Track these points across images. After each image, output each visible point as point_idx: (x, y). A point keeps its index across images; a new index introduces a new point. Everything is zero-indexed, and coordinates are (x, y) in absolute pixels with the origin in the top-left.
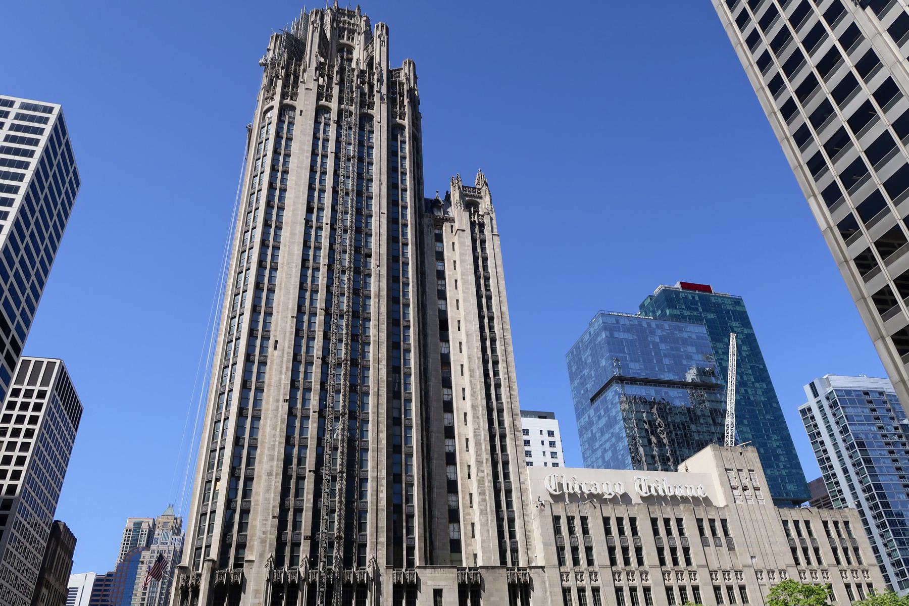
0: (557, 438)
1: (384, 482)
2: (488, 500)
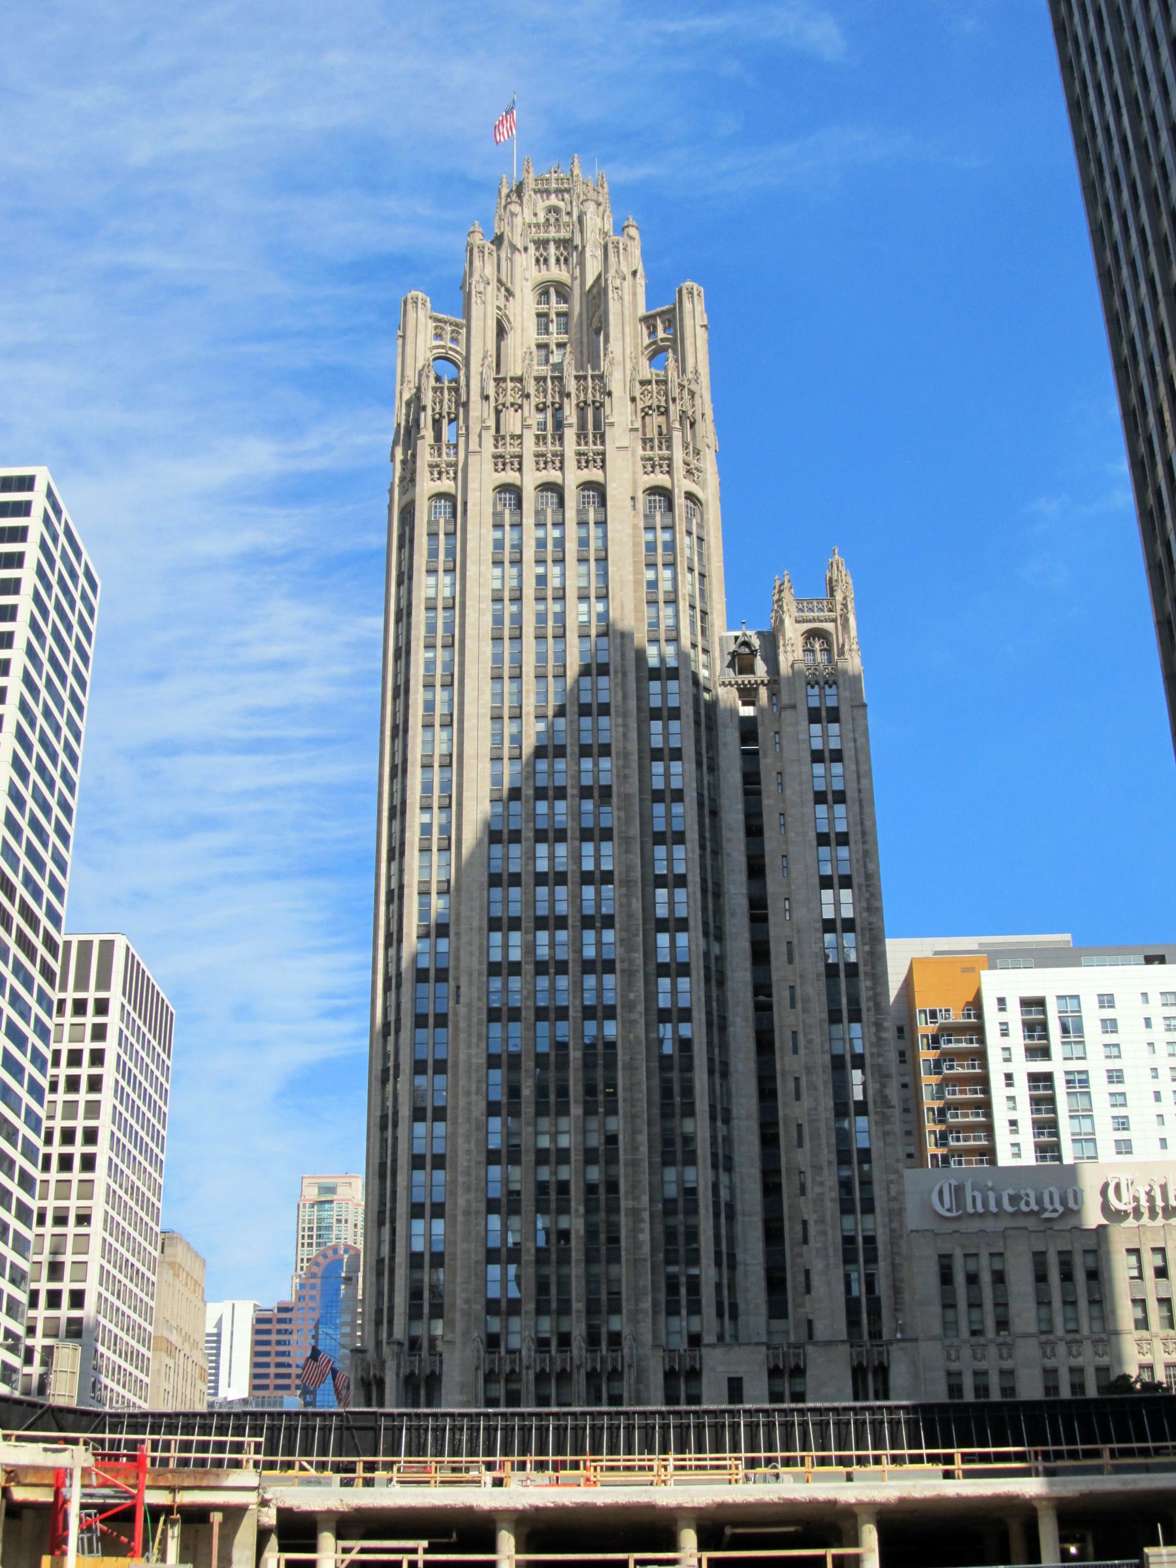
1: (646, 1215)
2: (830, 1232)
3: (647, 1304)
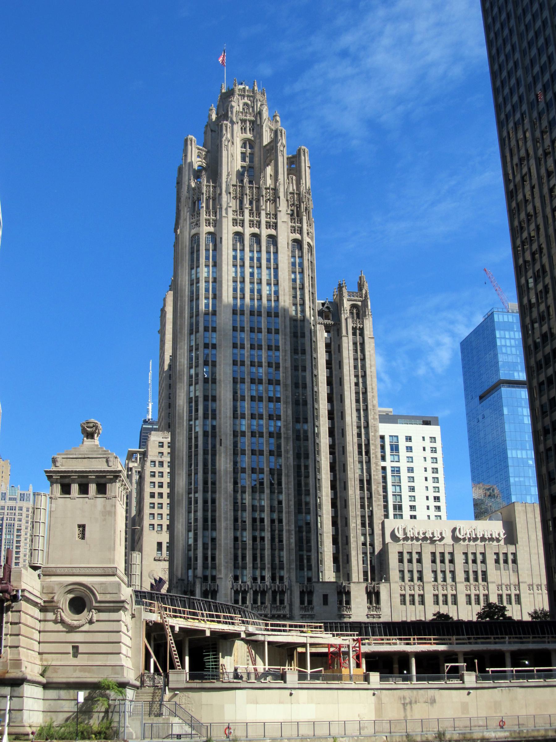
0: (438, 445)
1: (293, 532)
3: (293, 566)
